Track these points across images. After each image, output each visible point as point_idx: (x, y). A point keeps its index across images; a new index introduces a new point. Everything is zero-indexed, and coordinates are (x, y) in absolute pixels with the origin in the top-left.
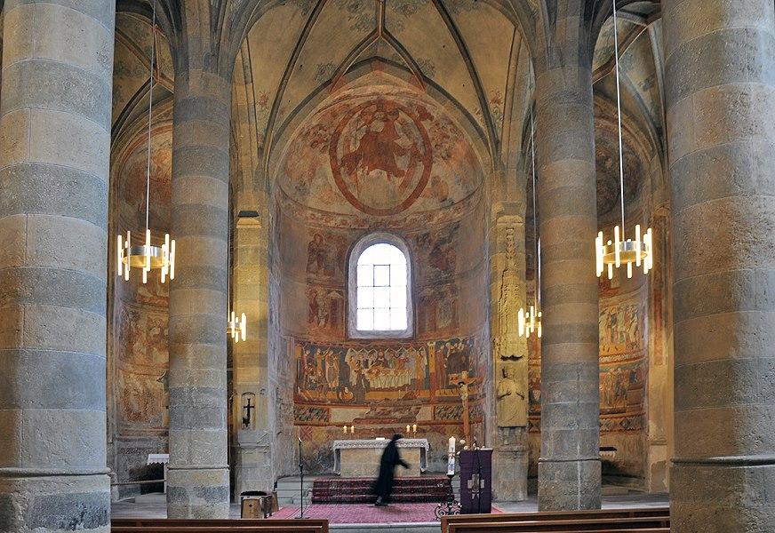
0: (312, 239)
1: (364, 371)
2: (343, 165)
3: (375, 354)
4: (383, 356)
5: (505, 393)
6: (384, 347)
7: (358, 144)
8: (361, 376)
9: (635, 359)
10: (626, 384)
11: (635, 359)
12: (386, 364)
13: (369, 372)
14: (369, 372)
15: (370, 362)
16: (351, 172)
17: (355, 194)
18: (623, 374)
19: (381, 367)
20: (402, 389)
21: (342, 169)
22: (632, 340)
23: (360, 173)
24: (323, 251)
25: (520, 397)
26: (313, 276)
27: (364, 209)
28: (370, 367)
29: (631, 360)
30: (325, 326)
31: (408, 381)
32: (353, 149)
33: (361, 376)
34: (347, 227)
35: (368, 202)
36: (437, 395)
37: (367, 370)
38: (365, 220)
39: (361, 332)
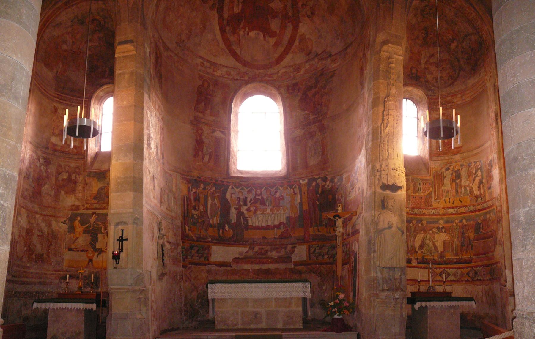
0: (201, 83)
1: (244, 209)
2: (228, 25)
3: (254, 192)
4: (260, 194)
5: (386, 226)
6: (257, 186)
7: (240, 6)
8: (240, 214)
9: (480, 210)
10: (471, 234)
11: (480, 210)
12: (263, 203)
13: (248, 210)
14: (248, 210)
15: (249, 200)
16: (234, 32)
17: (238, 51)
18: (468, 225)
19: (259, 206)
20: (278, 226)
21: (228, 28)
22: (476, 192)
23: (241, 33)
24: (210, 95)
25: (400, 233)
26: (201, 115)
27: (245, 64)
28: (249, 204)
29: (475, 211)
30: (209, 162)
31: (283, 219)
32: (236, 10)
33: (240, 214)
34: (231, 77)
35: (248, 58)
36: (311, 233)
37: (245, 207)
38: (245, 73)
39: (241, 172)
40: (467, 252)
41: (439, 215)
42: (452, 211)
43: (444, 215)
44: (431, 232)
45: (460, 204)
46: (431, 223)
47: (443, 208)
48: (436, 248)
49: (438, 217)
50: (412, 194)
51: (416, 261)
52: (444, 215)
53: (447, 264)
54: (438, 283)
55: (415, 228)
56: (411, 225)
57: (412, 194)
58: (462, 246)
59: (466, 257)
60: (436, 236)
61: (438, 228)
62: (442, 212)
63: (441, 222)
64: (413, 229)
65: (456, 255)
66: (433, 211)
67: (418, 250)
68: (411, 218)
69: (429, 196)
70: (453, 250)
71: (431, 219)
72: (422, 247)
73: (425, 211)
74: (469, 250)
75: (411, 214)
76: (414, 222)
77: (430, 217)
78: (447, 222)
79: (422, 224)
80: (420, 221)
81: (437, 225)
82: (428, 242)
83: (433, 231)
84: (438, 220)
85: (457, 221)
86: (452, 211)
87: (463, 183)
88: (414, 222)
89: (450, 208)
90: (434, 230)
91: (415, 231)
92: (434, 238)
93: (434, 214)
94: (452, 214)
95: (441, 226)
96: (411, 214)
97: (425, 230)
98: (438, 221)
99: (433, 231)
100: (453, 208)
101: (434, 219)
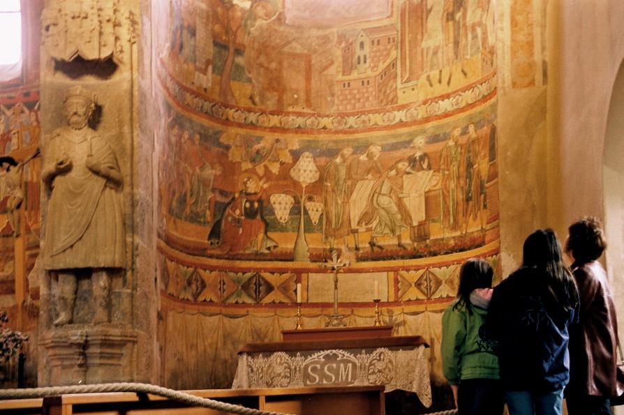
40: (475, 218)
41: (415, 122)
42: (446, 105)
43: (427, 120)
44: (393, 172)
45: (464, 82)
46: (394, 147)
47: (425, 103)
48: (406, 216)
49: (413, 128)
50: (340, 77)
51: (352, 255)
52: (427, 120)
53: (435, 254)
54: (413, 308)
55: (349, 169)
56: (338, 160)
57: (340, 77)
58: (468, 199)
59: (473, 228)
60: (406, 180)
61: (412, 161)
62: (421, 113)
63: (420, 141)
64: (343, 172)
65: (455, 226)
66: (400, 115)
67: (359, 223)
68: (336, 142)
69: (388, 74)
70: (446, 214)
71: (394, 136)
72: (366, 218)
73: (377, 119)
74: (479, 209)
75: (337, 132)
76: (347, 151)
77: (393, 132)
78: (435, 139)
79: (370, 156)
80: (362, 147)
81: (408, 152)
82: (384, 201)
83: (397, 170)
84: (413, 136)
85: (457, 132)
86: (446, 105)
87: (470, 19)
88: (347, 151)
89: (443, 97)
90: (400, 165)
91: (349, 176)
92: (402, 187)
93: (402, 124)
94: (447, 115)
95: (418, 154)
96: (337, 132)
97: (375, 169)
98: (411, 141)
99: (397, 170)
100: (448, 96)
101: (401, 135)
